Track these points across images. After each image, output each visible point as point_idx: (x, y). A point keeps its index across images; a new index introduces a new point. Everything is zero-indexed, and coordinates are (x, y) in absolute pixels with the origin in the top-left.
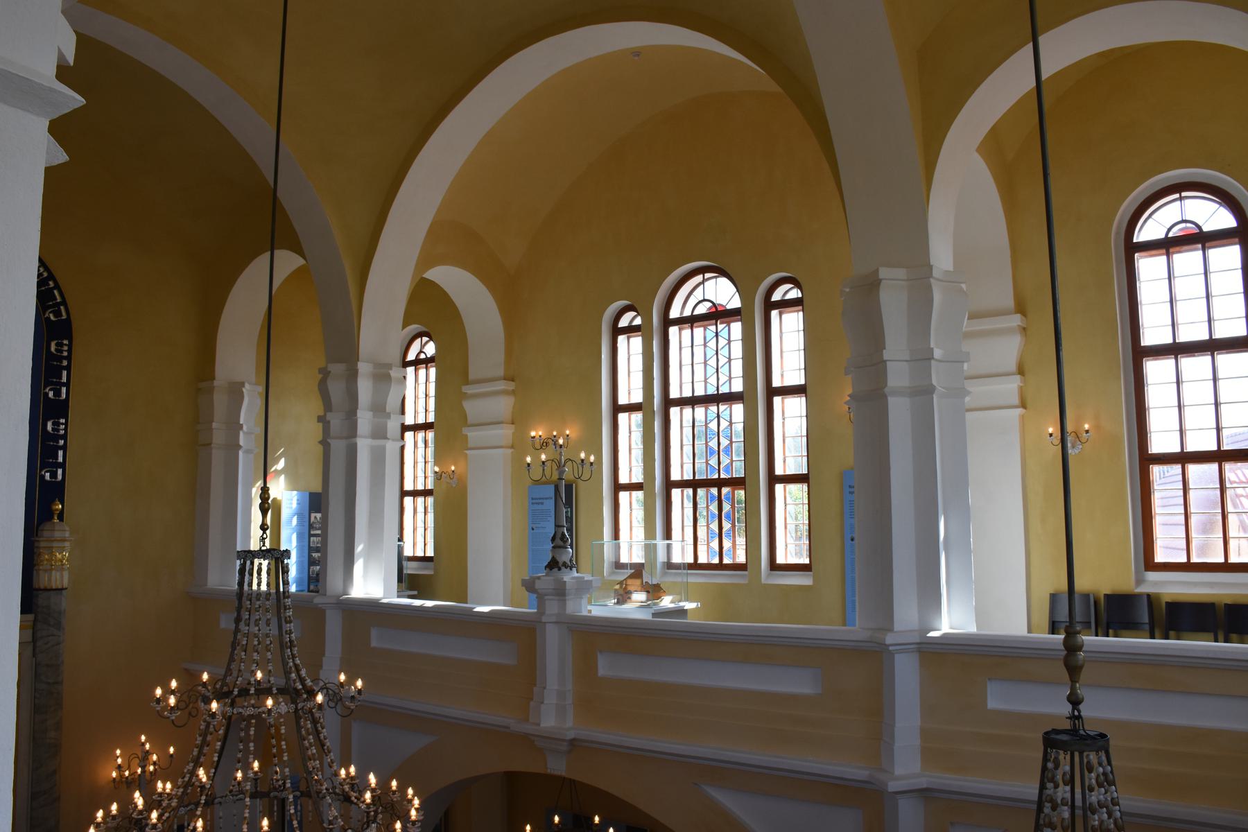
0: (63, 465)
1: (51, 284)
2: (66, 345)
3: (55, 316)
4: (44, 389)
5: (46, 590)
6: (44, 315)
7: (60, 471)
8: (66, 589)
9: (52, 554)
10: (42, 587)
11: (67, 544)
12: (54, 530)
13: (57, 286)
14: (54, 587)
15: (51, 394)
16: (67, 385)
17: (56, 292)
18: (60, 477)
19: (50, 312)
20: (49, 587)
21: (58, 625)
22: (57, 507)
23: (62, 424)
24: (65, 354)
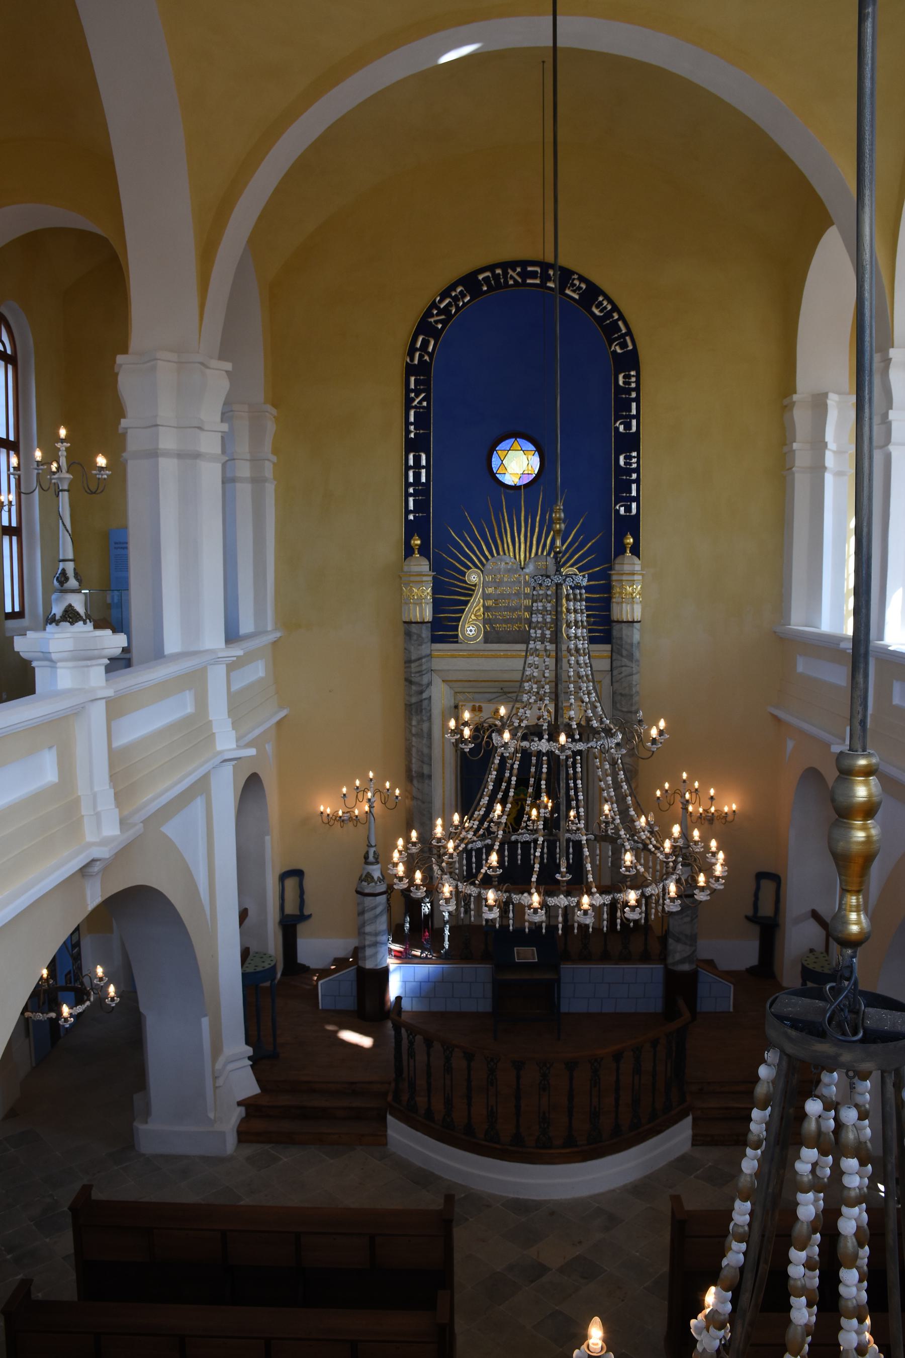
0: (637, 499)
1: (616, 316)
2: (633, 376)
3: (621, 349)
4: (615, 424)
5: (618, 622)
6: (610, 348)
7: (634, 505)
8: (640, 622)
9: (622, 587)
10: (615, 620)
11: (636, 577)
12: (623, 564)
13: (622, 317)
14: (625, 620)
15: (621, 429)
16: (637, 417)
17: (620, 323)
18: (634, 511)
19: (616, 345)
20: (620, 620)
21: (631, 657)
22: (628, 541)
23: (634, 457)
24: (633, 385)
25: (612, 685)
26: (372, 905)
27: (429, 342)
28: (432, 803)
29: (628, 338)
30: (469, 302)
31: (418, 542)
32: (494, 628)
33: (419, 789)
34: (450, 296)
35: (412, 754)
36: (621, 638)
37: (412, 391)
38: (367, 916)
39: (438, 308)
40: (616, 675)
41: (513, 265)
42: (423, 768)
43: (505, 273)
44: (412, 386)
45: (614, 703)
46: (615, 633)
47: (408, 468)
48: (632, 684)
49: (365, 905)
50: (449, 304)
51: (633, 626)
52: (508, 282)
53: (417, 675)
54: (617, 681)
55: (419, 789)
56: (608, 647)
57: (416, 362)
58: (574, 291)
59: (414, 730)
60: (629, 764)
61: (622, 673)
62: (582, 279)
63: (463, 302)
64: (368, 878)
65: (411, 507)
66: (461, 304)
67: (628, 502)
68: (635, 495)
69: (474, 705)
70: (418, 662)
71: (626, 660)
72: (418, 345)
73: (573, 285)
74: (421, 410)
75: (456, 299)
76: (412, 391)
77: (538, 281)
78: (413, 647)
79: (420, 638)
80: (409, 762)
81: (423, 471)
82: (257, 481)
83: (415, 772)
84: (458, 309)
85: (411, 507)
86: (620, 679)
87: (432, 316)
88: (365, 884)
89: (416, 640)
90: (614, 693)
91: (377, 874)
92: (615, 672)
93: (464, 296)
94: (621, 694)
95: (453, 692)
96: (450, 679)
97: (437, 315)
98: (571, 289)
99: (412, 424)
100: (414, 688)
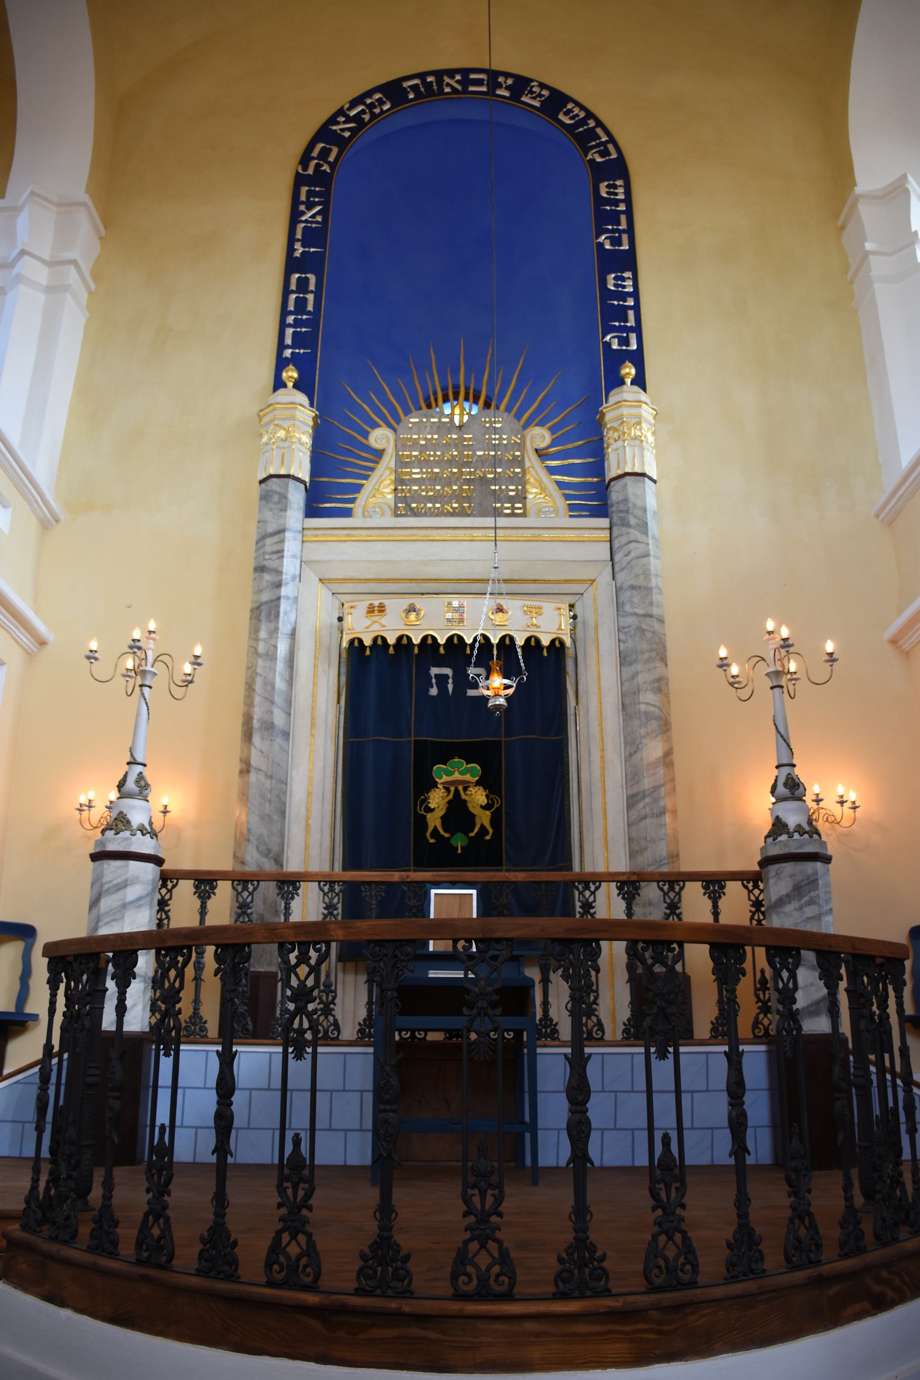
3: (602, 156)
8: (655, 481)
13: (599, 124)
21: (643, 527)
25: (614, 579)
26: (119, 880)
27: (330, 150)
28: (286, 784)
29: (611, 147)
30: (388, 110)
31: (295, 375)
32: (412, 509)
33: (262, 752)
34: (365, 104)
35: (254, 690)
36: (626, 500)
37: (303, 203)
38: (105, 904)
39: (347, 116)
40: (620, 560)
41: (451, 73)
42: (272, 712)
43: (440, 81)
44: (303, 198)
45: (619, 605)
46: (615, 494)
47: (286, 292)
48: (649, 569)
49: (105, 879)
50: (363, 112)
51: (644, 482)
52: (444, 90)
53: (275, 556)
54: (623, 569)
55: (262, 752)
56: (604, 522)
57: (310, 171)
58: (534, 98)
59: (261, 648)
60: (654, 706)
61: (630, 552)
62: (542, 86)
63: (382, 109)
64: (119, 822)
65: (288, 341)
66: (377, 111)
67: (622, 333)
68: (634, 325)
69: (371, 604)
70: (278, 536)
71: (636, 532)
72: (315, 153)
73: (531, 92)
74: (314, 225)
75: (371, 106)
76: (303, 203)
77: (484, 89)
78: (270, 513)
79: (284, 500)
80: (249, 703)
81: (311, 297)
82: (53, 289)
83: (259, 721)
84: (373, 116)
85: (288, 341)
86: (628, 564)
87: (338, 123)
88: (111, 833)
89: (278, 503)
90: (618, 590)
91: (137, 818)
92: (617, 558)
93: (384, 103)
94: (633, 587)
95: (337, 604)
96: (333, 577)
97: (344, 123)
98: (529, 96)
99: (298, 240)
100: (267, 577)
